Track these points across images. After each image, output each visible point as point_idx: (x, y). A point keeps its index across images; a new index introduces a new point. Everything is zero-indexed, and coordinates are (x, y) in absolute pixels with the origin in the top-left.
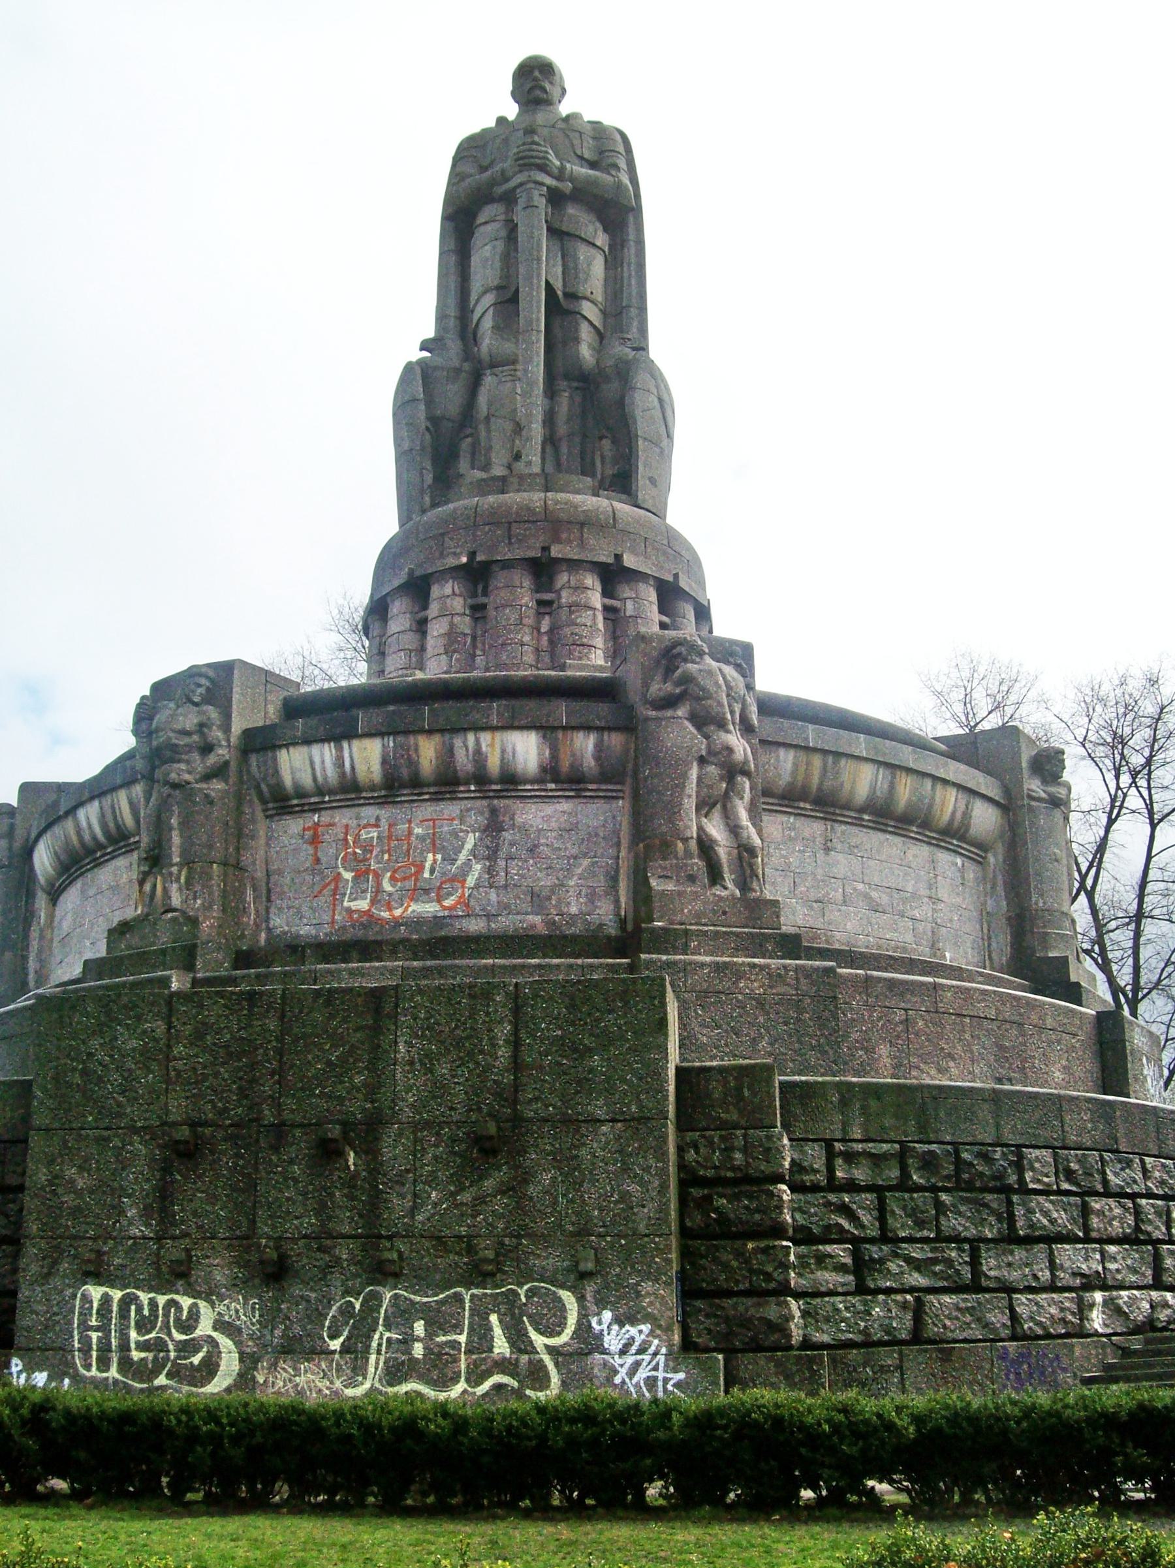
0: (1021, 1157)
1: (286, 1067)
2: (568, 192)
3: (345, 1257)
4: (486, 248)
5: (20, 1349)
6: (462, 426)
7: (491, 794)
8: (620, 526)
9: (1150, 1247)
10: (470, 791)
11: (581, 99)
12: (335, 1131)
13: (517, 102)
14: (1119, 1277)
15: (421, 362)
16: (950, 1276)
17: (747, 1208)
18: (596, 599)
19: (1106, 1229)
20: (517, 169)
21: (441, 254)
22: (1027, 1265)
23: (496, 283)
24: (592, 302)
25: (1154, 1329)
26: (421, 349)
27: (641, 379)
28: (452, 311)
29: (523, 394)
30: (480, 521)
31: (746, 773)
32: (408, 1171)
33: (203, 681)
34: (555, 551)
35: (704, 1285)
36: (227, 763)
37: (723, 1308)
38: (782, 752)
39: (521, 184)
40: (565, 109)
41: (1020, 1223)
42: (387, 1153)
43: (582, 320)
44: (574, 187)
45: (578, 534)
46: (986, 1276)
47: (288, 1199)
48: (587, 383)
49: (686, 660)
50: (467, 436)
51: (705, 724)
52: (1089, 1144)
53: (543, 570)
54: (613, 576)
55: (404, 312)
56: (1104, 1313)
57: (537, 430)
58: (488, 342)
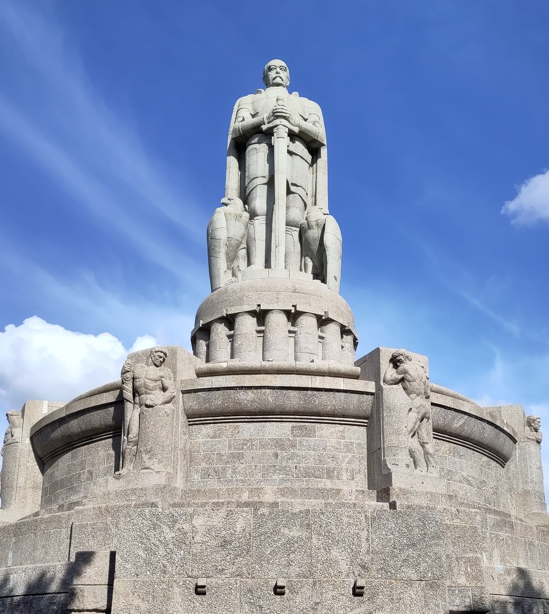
33: (162, 355)
39: (276, 126)
50: (242, 249)
53: (293, 316)
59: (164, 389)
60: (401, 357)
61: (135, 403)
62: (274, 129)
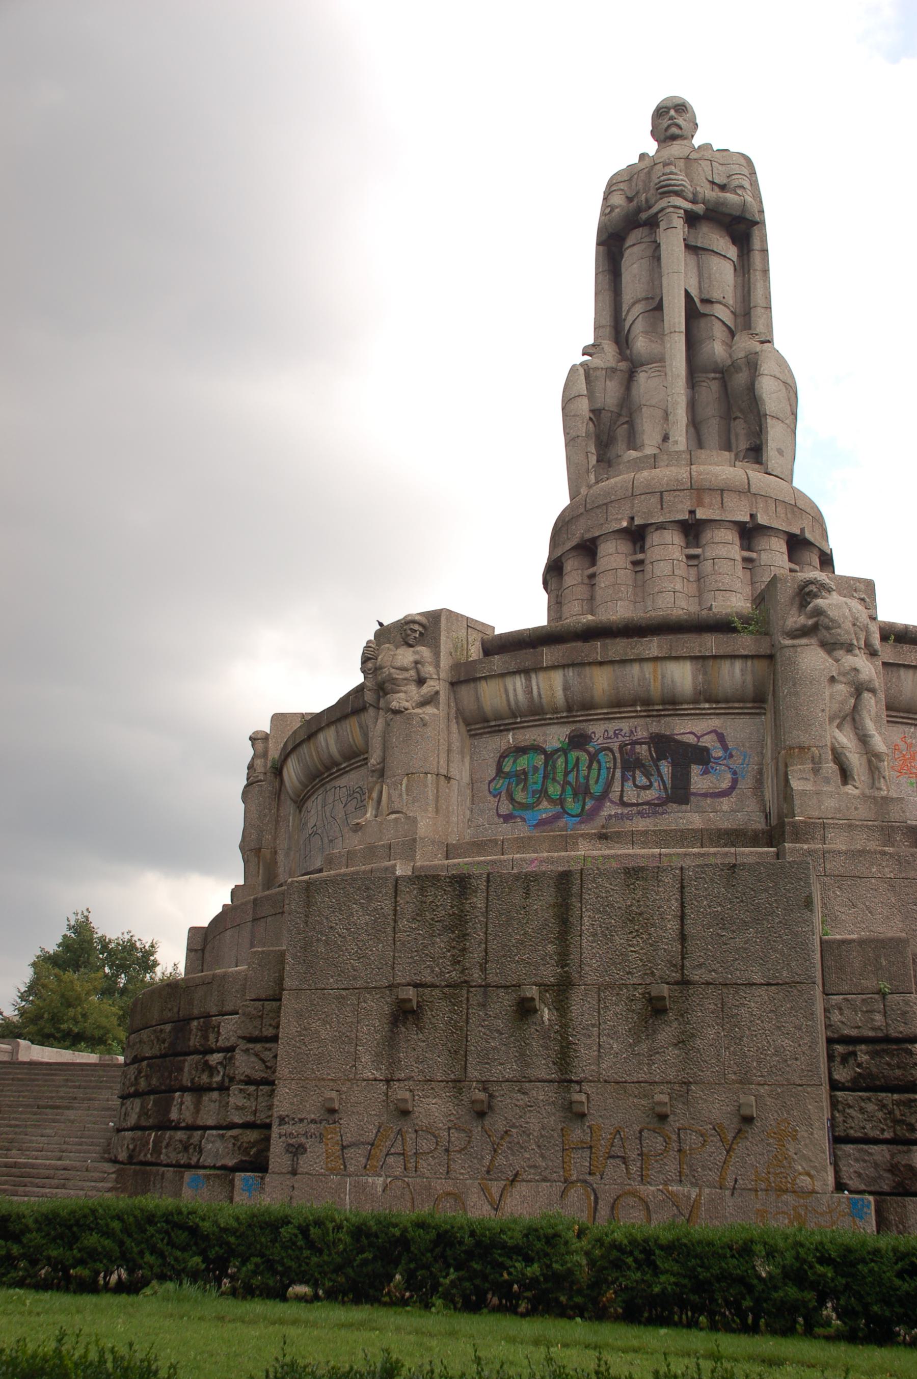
1: (490, 938)
2: (701, 212)
3: (541, 1098)
4: (635, 266)
5: (273, 1173)
6: (619, 415)
7: (655, 713)
8: (753, 490)
10: (636, 711)
11: (712, 132)
12: (532, 992)
13: (656, 141)
15: (582, 364)
17: (889, 1064)
18: (736, 552)
20: (659, 196)
21: (596, 274)
23: (644, 295)
24: (725, 305)
26: (584, 354)
27: (767, 367)
28: (607, 320)
29: (668, 388)
30: (637, 492)
31: (873, 691)
32: (593, 1026)
33: (416, 627)
34: (700, 514)
35: (852, 1132)
36: (437, 693)
37: (871, 1154)
38: (902, 672)
39: (662, 210)
40: (697, 141)
42: (575, 1009)
43: (716, 322)
44: (707, 209)
45: (719, 499)
47: (494, 1049)
48: (724, 373)
49: (816, 596)
50: (623, 424)
51: (834, 649)
53: (692, 530)
54: (750, 533)
55: (569, 322)
57: (681, 415)
58: (641, 344)
59: (421, 681)
60: (813, 588)
61: (378, 709)
62: (660, 215)
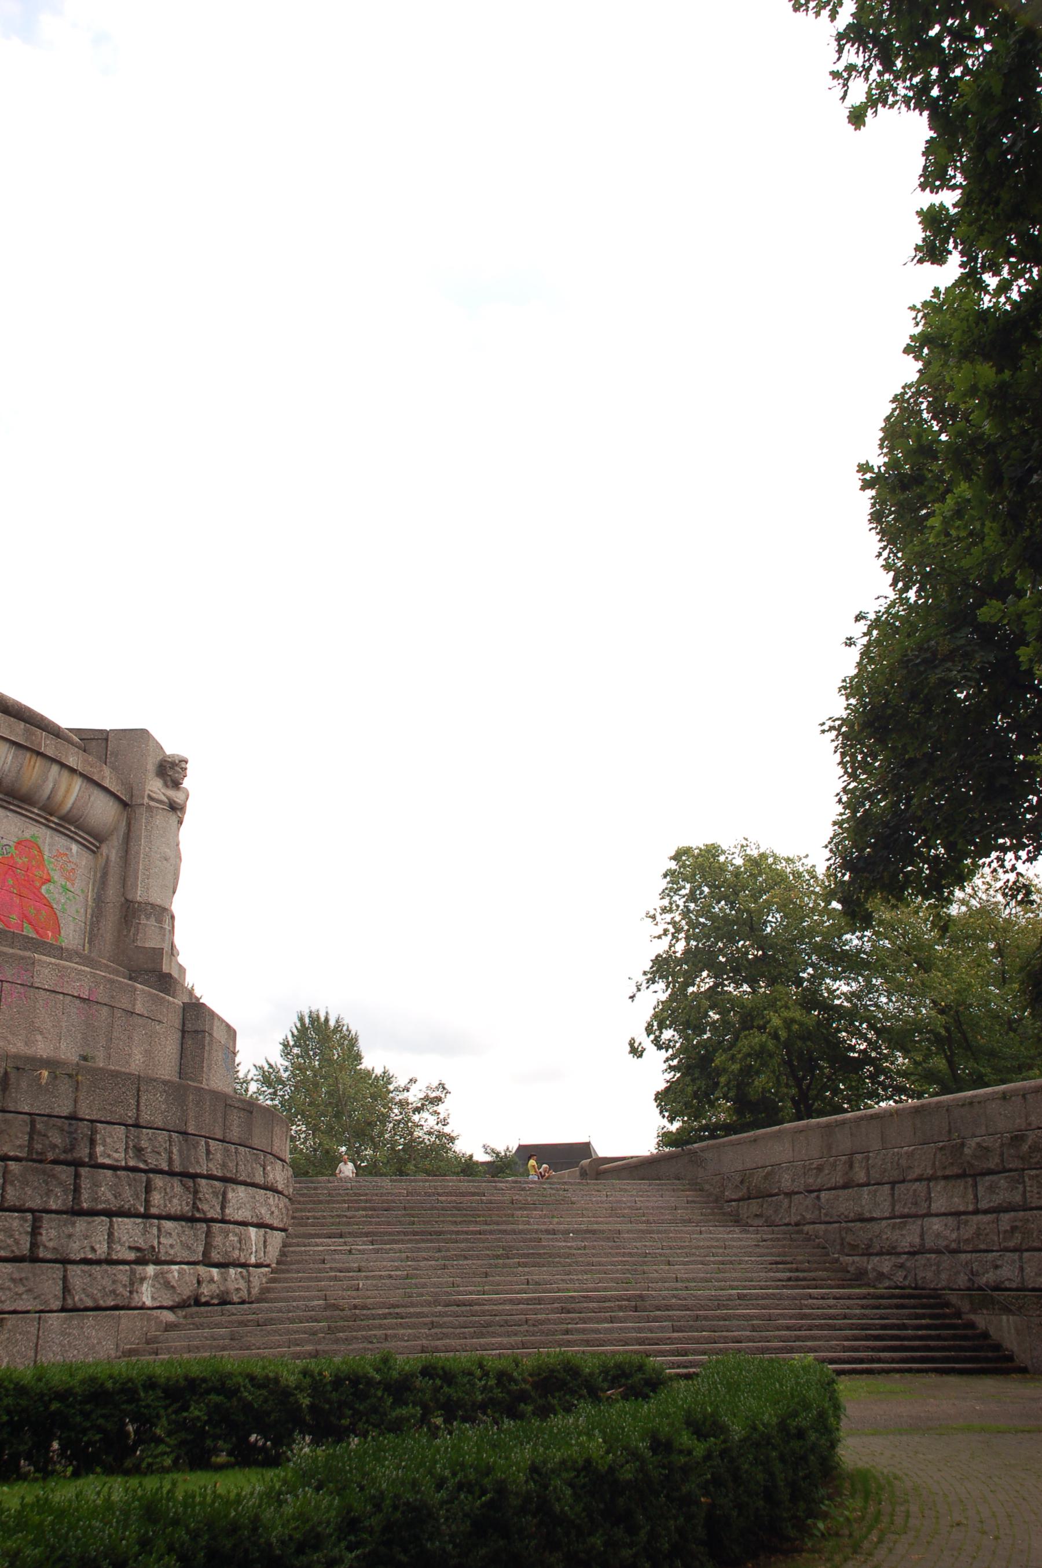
0: (94, 1132)
9: (204, 1225)
14: (172, 1252)
16: (9, 1246)
19: (165, 1206)
22: (86, 1237)
25: (197, 1303)
41: (85, 1195)
46: (45, 1247)
52: (160, 1124)
56: (153, 1286)
